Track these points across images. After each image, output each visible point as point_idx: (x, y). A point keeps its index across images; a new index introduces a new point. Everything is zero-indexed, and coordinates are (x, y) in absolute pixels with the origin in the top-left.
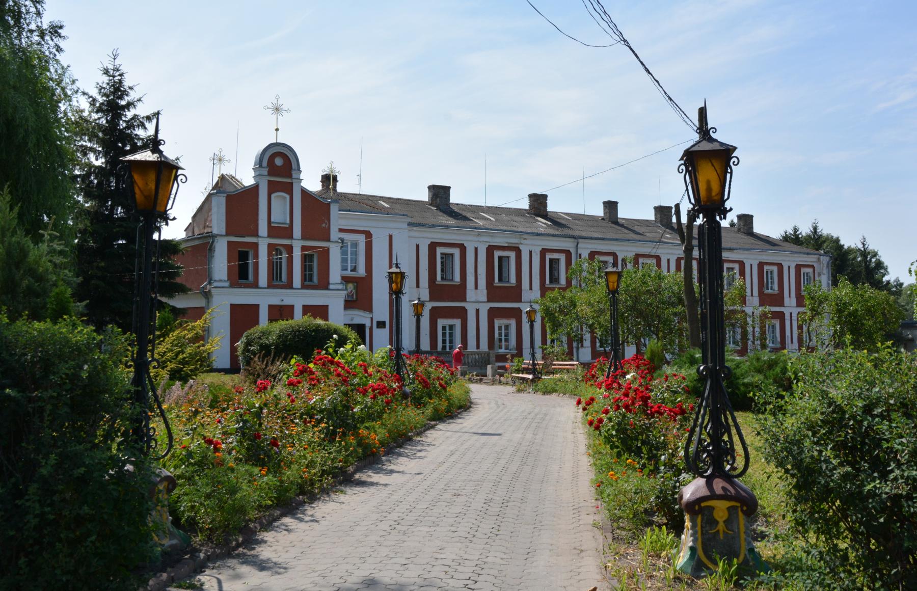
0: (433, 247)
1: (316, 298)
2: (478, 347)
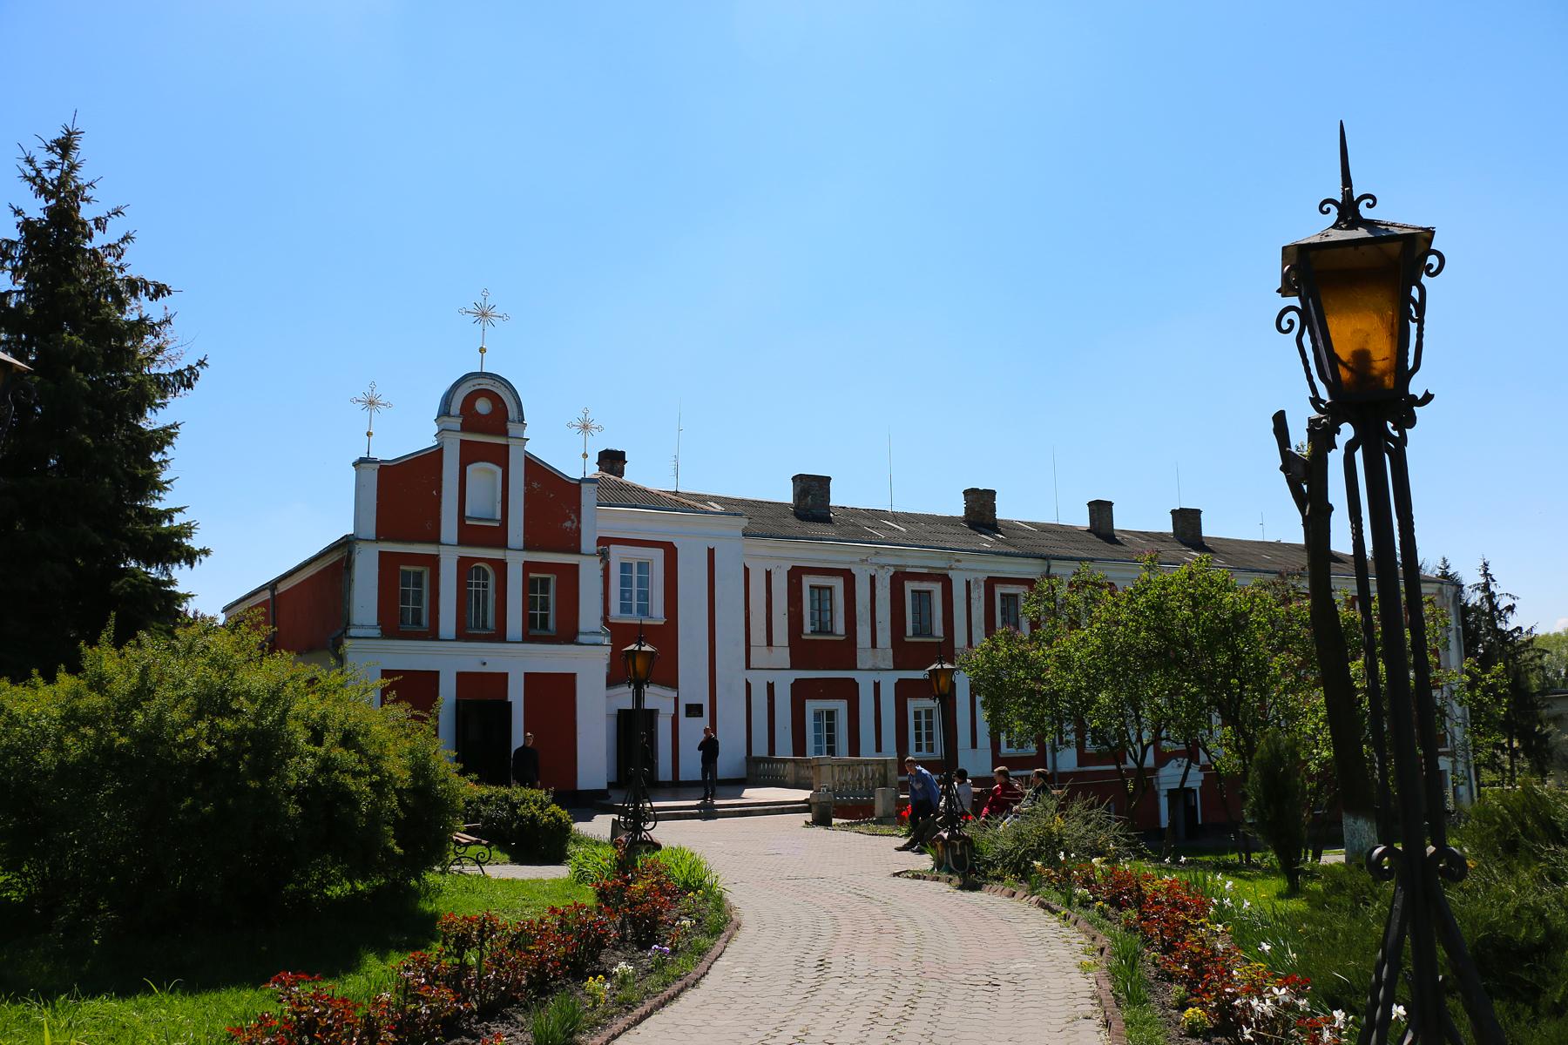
0: (796, 574)
1: (550, 659)
2: (879, 749)
